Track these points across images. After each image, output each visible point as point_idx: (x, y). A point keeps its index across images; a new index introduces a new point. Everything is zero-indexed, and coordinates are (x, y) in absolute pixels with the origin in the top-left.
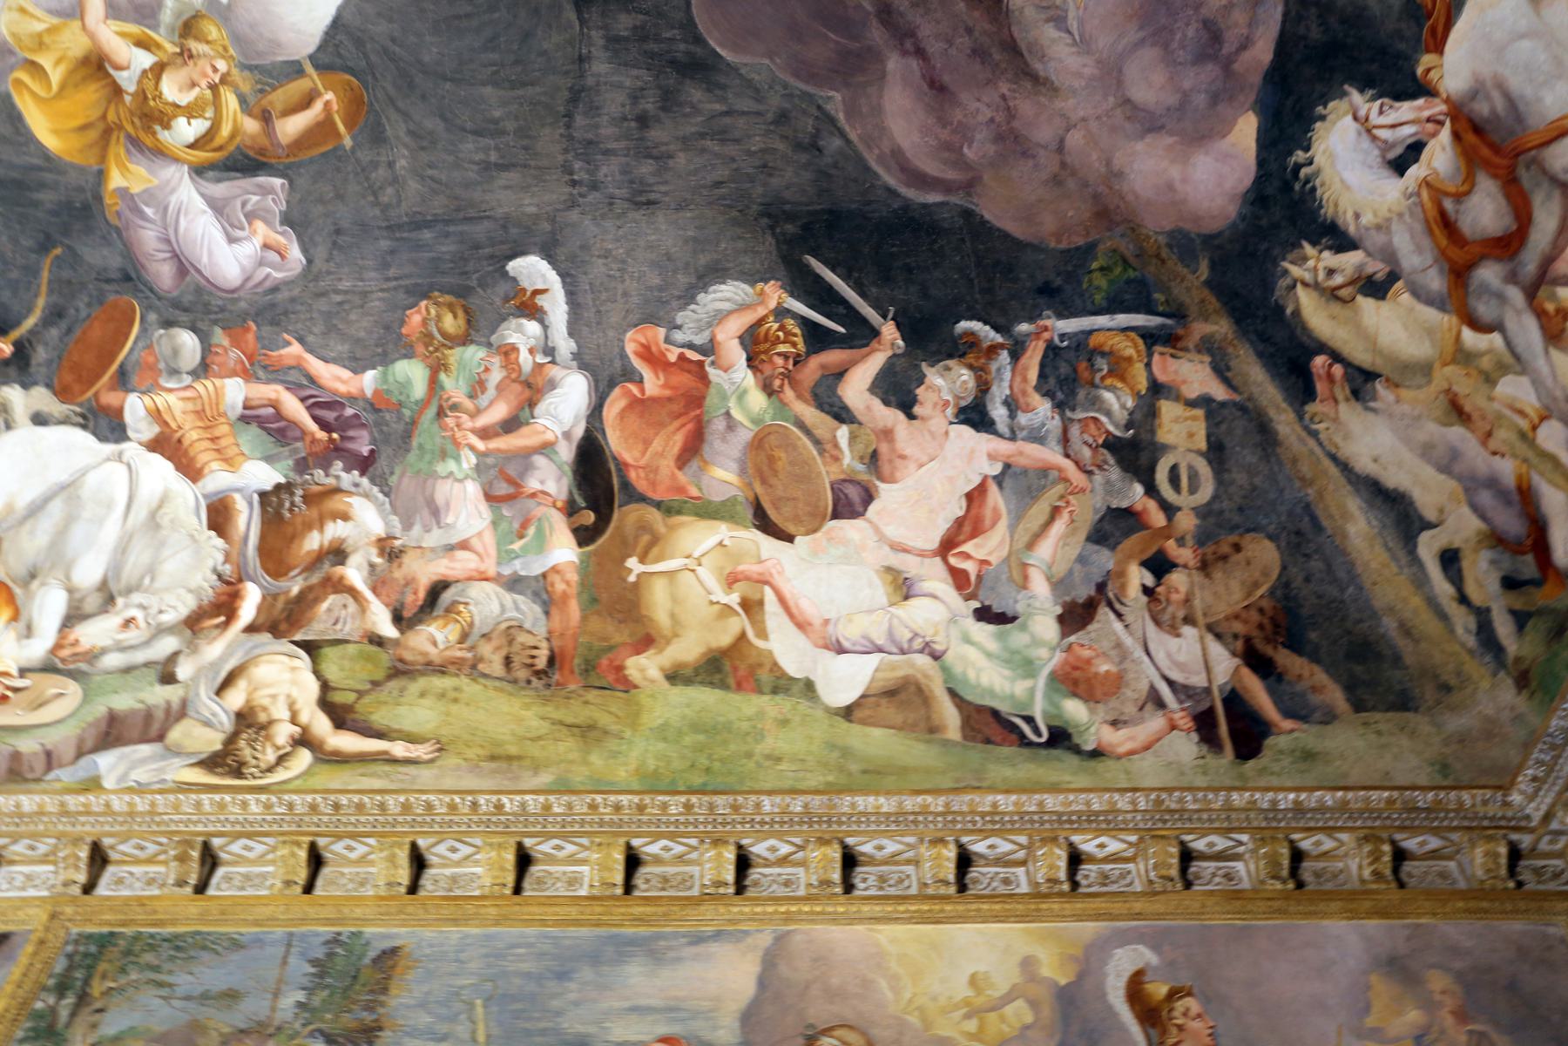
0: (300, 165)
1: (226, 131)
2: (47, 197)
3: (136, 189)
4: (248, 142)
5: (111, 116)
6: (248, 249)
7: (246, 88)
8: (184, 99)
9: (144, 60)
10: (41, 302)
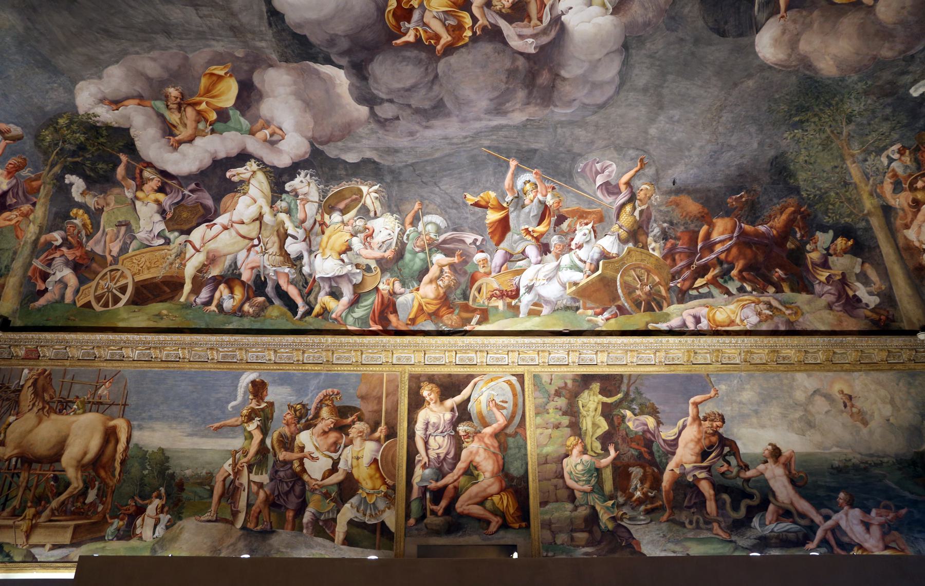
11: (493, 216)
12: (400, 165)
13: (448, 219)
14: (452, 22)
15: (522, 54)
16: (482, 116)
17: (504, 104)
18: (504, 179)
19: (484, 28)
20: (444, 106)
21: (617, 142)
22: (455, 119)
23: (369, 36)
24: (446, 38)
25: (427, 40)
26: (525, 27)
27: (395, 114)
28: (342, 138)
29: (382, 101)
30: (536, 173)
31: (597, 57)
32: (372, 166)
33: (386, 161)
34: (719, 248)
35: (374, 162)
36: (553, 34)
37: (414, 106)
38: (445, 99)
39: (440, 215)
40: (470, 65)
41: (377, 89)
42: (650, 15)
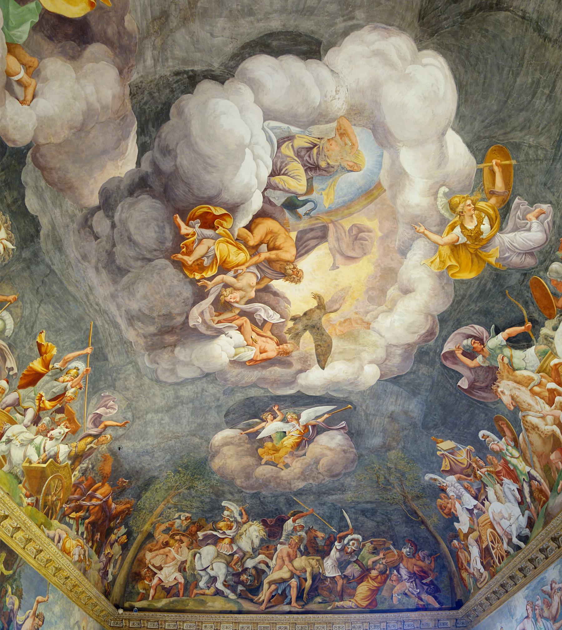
0: (514, 187)
1: (491, 212)
2: (489, 285)
3: (498, 255)
4: (498, 205)
5: (472, 251)
6: (535, 225)
7: (480, 196)
8: (475, 222)
9: (458, 230)
10: (520, 306)
11: (37, 365)
12: (47, 259)
13: (15, 333)
14: (206, 262)
15: (187, 318)
16: (123, 309)
17: (139, 319)
18: (73, 351)
19: (204, 287)
20: (123, 276)
21: (134, 403)
22: (113, 289)
23: (180, 191)
24: (189, 260)
25: (185, 245)
26: (211, 314)
27: (100, 234)
28: (51, 183)
29: (111, 217)
30: (87, 370)
31: (196, 363)
32: (32, 231)
33: (44, 243)
34: (94, 502)
35: (38, 231)
36: (209, 333)
37: (114, 249)
38: (130, 275)
39: (15, 324)
40: (168, 284)
41: (122, 208)
42: (233, 379)
